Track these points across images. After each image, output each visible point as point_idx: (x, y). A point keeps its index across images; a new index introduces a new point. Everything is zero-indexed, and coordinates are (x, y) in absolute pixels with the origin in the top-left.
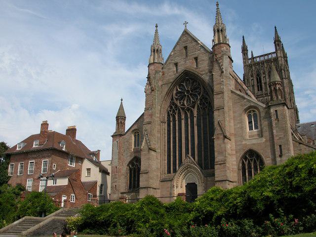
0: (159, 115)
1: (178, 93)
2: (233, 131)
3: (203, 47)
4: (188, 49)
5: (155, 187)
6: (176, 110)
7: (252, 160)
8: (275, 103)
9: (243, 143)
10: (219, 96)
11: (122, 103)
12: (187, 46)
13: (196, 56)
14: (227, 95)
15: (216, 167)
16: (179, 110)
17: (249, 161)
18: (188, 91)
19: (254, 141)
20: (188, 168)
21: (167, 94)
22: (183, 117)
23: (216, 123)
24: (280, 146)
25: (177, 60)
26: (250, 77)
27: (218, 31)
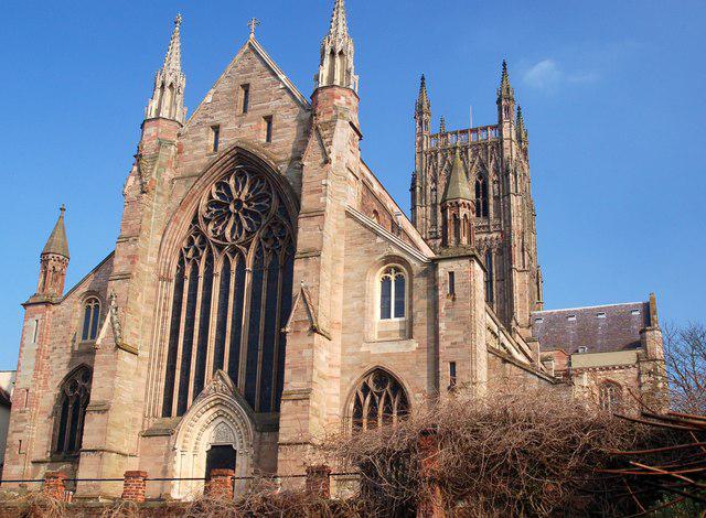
0: (155, 259)
1: (212, 203)
2: (339, 317)
4: (251, 91)
5: (126, 451)
6: (203, 249)
7: (380, 395)
8: (450, 252)
9: (363, 349)
10: (313, 223)
13: (268, 112)
14: (334, 223)
15: (285, 406)
16: (210, 251)
17: (373, 399)
18: (238, 203)
19: (392, 348)
21: (183, 205)
22: (218, 268)
23: (296, 291)
24: (453, 364)
25: (219, 117)
26: (429, 182)
27: (333, 53)
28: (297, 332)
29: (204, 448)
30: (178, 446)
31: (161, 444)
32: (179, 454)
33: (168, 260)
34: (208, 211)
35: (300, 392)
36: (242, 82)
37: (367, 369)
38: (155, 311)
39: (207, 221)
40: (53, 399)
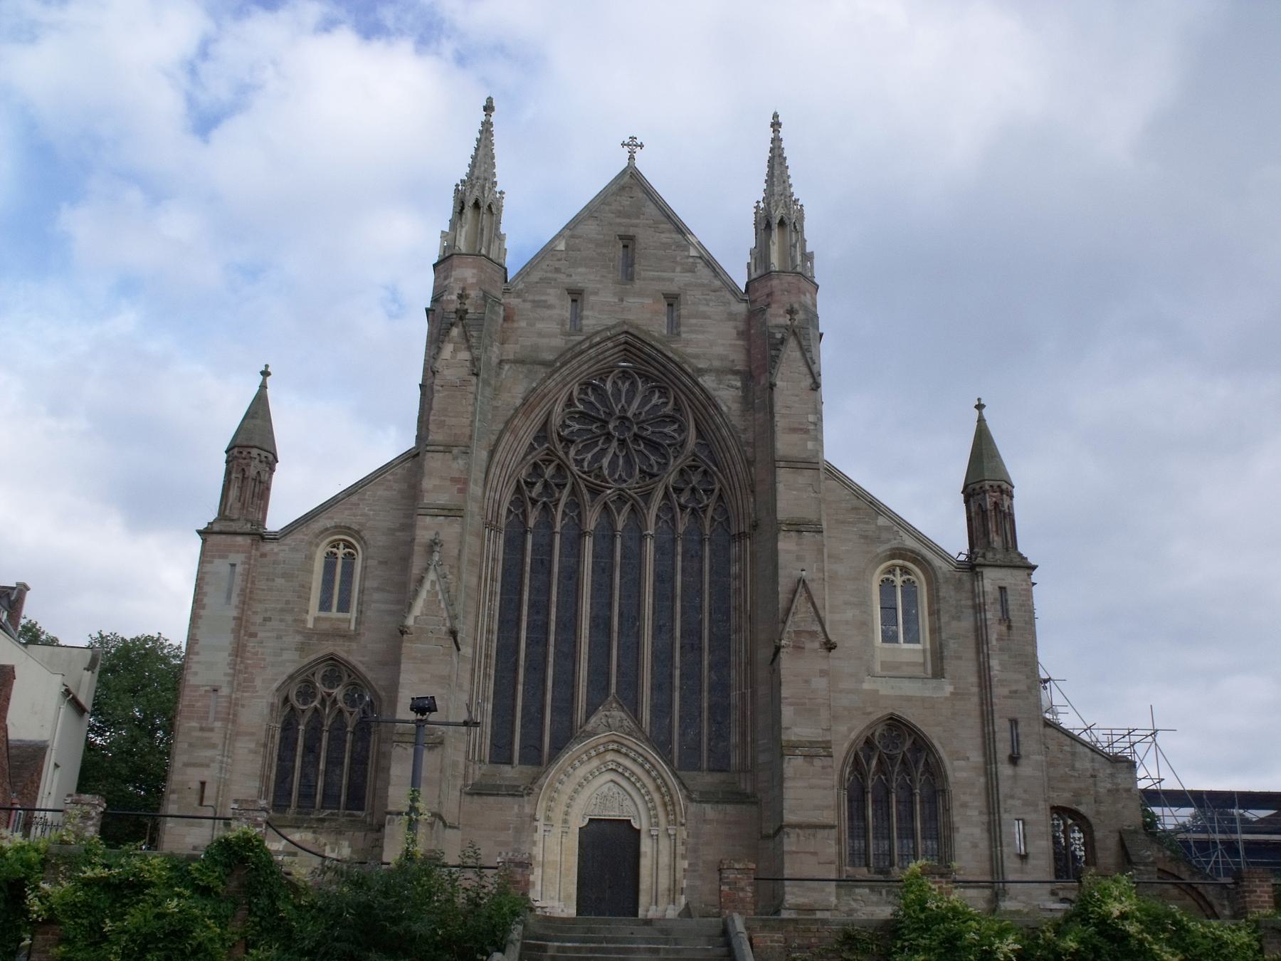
3: (710, 263)
6: (561, 486)
9: (866, 686)
11: (263, 387)
12: (632, 238)
13: (673, 288)
17: (880, 761)
20: (607, 751)
22: (592, 520)
24: (1014, 723)
25: (581, 277)
28: (799, 648)
29: (578, 821)
30: (540, 815)
31: (512, 809)
32: (540, 825)
33: (497, 497)
34: (564, 426)
35: (812, 744)
36: (622, 231)
37: (874, 717)
38: (480, 578)
39: (567, 442)
40: (266, 711)
